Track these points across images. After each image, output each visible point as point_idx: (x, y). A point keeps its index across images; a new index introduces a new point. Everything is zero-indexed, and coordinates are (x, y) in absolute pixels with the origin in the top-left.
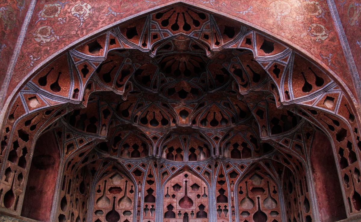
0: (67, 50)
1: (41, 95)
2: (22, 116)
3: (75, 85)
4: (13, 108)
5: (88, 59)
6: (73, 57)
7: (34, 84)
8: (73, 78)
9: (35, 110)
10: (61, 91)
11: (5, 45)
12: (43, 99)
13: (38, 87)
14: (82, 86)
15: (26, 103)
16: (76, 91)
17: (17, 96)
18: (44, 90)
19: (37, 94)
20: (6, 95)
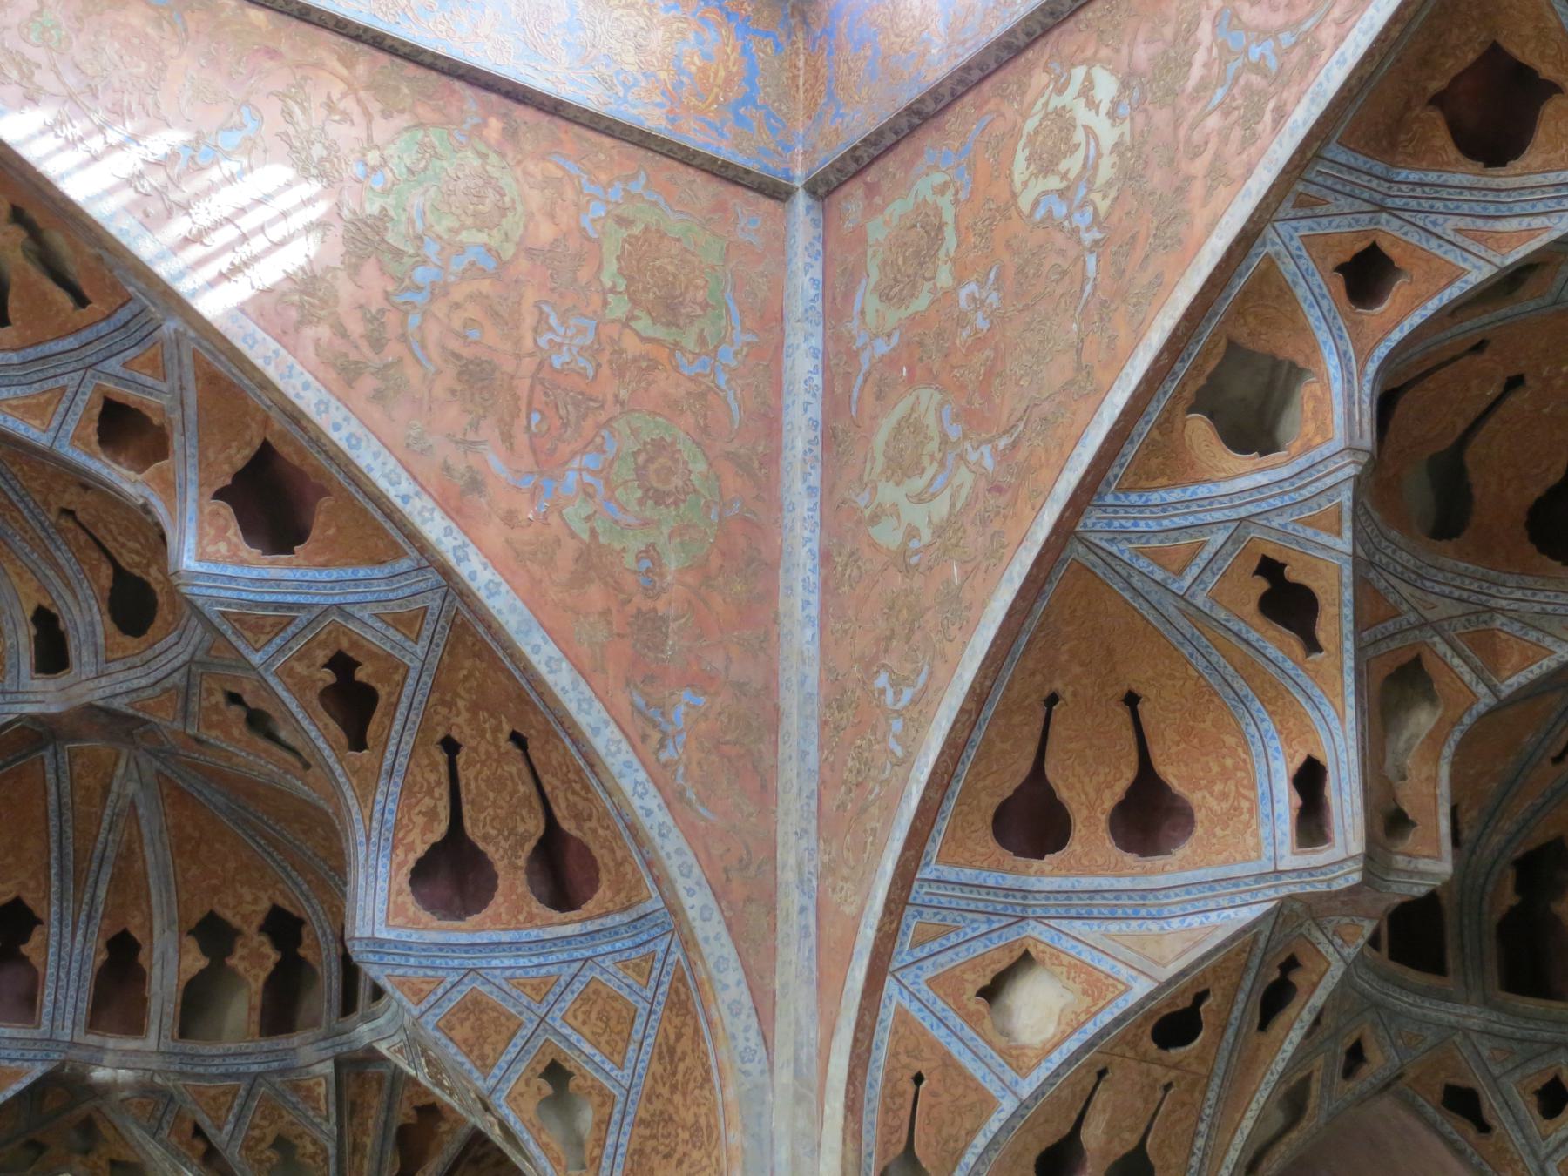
0: (1064, 531)
1: (1064, 925)
2: (980, 1142)
3: (1288, 741)
4: (887, 1110)
5: (1252, 509)
6: (1140, 552)
7: (967, 875)
8: (1245, 690)
9: (1057, 1058)
10: (1199, 830)
11: (686, 695)
12: (1087, 956)
13: (1010, 881)
14: (1335, 724)
15: (968, 1032)
16: (1310, 779)
17: (887, 1014)
18: (1066, 884)
19: (1035, 931)
20: (813, 1033)
